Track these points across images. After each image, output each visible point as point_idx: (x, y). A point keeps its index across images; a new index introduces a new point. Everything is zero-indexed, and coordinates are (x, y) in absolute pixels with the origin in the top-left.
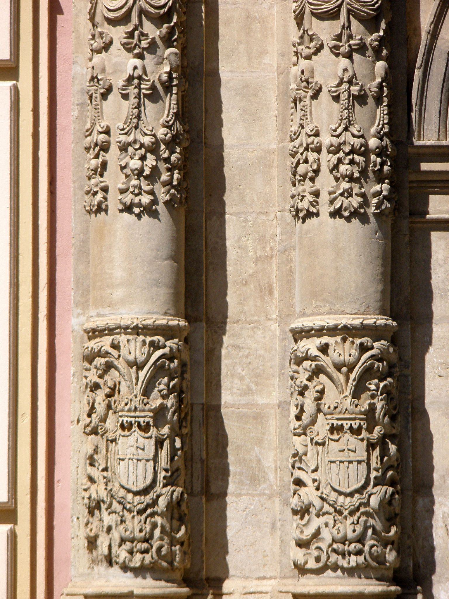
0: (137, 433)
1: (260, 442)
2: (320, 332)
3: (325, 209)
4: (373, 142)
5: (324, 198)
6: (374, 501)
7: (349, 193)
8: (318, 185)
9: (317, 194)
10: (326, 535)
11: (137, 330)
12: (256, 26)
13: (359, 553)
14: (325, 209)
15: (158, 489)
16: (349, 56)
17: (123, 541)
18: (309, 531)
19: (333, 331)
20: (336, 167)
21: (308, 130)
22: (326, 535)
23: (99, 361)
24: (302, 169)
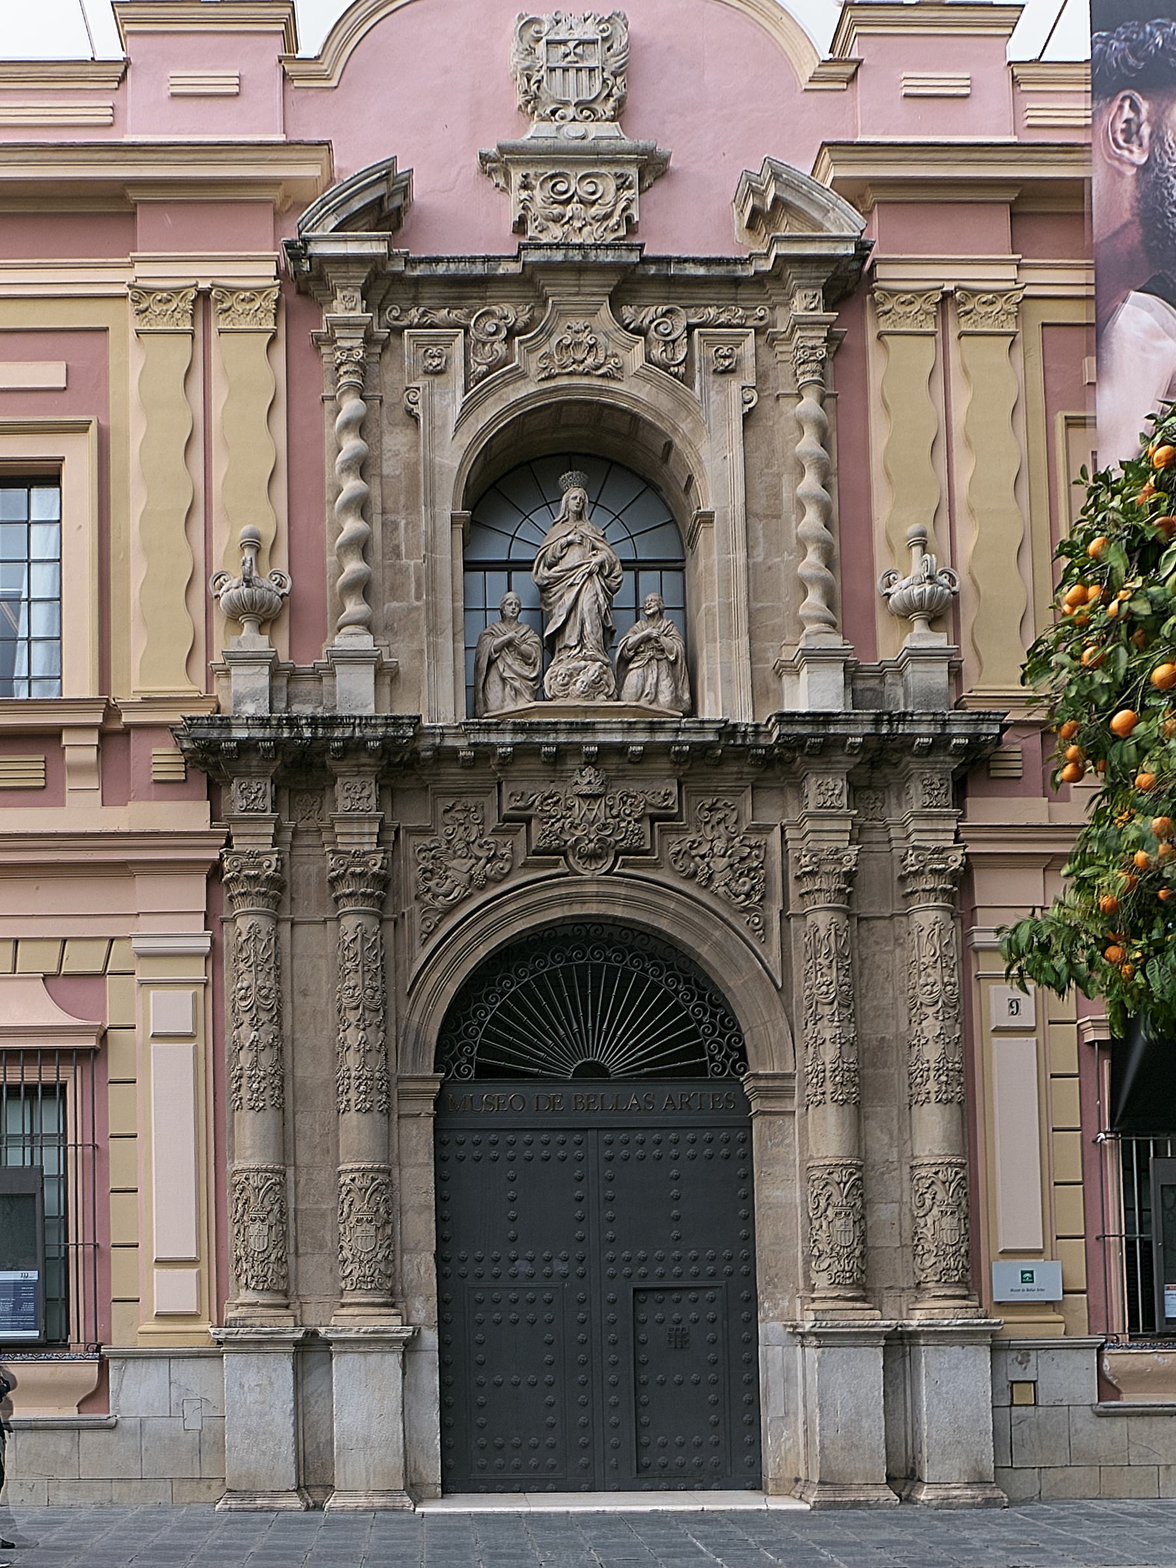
0: (258, 1224)
1: (324, 1227)
2: (351, 1171)
3: (353, 1110)
4: (377, 1075)
5: (352, 1103)
6: (380, 1256)
7: (365, 1100)
8: (349, 1095)
9: (348, 1101)
10: (356, 1274)
11: (258, 1171)
12: (319, 1015)
13: (372, 1282)
14: (353, 1110)
15: (270, 1249)
16: (364, 1030)
17: (253, 1278)
18: (347, 1272)
19: (358, 1170)
20: (358, 1087)
21: (344, 1068)
22: (356, 1274)
23: (240, 1187)
24: (341, 1089)
